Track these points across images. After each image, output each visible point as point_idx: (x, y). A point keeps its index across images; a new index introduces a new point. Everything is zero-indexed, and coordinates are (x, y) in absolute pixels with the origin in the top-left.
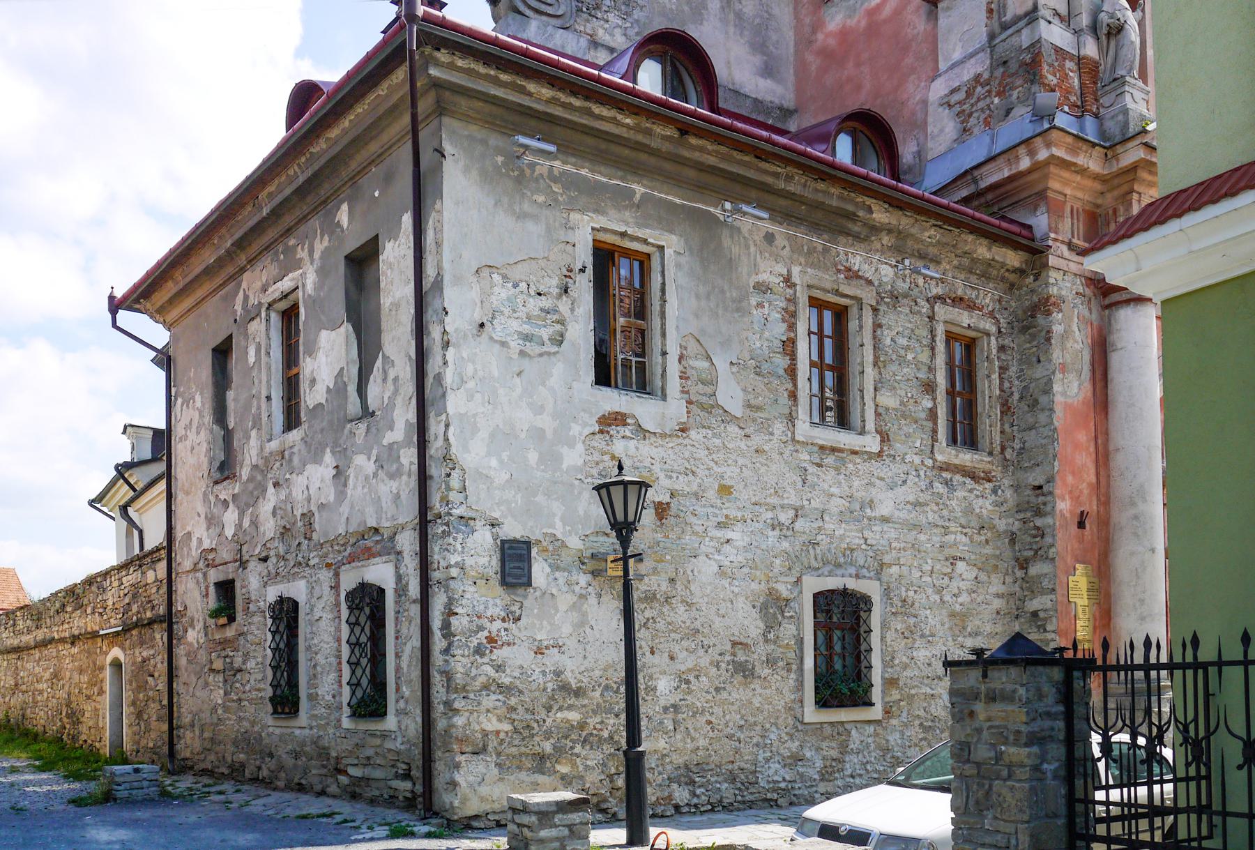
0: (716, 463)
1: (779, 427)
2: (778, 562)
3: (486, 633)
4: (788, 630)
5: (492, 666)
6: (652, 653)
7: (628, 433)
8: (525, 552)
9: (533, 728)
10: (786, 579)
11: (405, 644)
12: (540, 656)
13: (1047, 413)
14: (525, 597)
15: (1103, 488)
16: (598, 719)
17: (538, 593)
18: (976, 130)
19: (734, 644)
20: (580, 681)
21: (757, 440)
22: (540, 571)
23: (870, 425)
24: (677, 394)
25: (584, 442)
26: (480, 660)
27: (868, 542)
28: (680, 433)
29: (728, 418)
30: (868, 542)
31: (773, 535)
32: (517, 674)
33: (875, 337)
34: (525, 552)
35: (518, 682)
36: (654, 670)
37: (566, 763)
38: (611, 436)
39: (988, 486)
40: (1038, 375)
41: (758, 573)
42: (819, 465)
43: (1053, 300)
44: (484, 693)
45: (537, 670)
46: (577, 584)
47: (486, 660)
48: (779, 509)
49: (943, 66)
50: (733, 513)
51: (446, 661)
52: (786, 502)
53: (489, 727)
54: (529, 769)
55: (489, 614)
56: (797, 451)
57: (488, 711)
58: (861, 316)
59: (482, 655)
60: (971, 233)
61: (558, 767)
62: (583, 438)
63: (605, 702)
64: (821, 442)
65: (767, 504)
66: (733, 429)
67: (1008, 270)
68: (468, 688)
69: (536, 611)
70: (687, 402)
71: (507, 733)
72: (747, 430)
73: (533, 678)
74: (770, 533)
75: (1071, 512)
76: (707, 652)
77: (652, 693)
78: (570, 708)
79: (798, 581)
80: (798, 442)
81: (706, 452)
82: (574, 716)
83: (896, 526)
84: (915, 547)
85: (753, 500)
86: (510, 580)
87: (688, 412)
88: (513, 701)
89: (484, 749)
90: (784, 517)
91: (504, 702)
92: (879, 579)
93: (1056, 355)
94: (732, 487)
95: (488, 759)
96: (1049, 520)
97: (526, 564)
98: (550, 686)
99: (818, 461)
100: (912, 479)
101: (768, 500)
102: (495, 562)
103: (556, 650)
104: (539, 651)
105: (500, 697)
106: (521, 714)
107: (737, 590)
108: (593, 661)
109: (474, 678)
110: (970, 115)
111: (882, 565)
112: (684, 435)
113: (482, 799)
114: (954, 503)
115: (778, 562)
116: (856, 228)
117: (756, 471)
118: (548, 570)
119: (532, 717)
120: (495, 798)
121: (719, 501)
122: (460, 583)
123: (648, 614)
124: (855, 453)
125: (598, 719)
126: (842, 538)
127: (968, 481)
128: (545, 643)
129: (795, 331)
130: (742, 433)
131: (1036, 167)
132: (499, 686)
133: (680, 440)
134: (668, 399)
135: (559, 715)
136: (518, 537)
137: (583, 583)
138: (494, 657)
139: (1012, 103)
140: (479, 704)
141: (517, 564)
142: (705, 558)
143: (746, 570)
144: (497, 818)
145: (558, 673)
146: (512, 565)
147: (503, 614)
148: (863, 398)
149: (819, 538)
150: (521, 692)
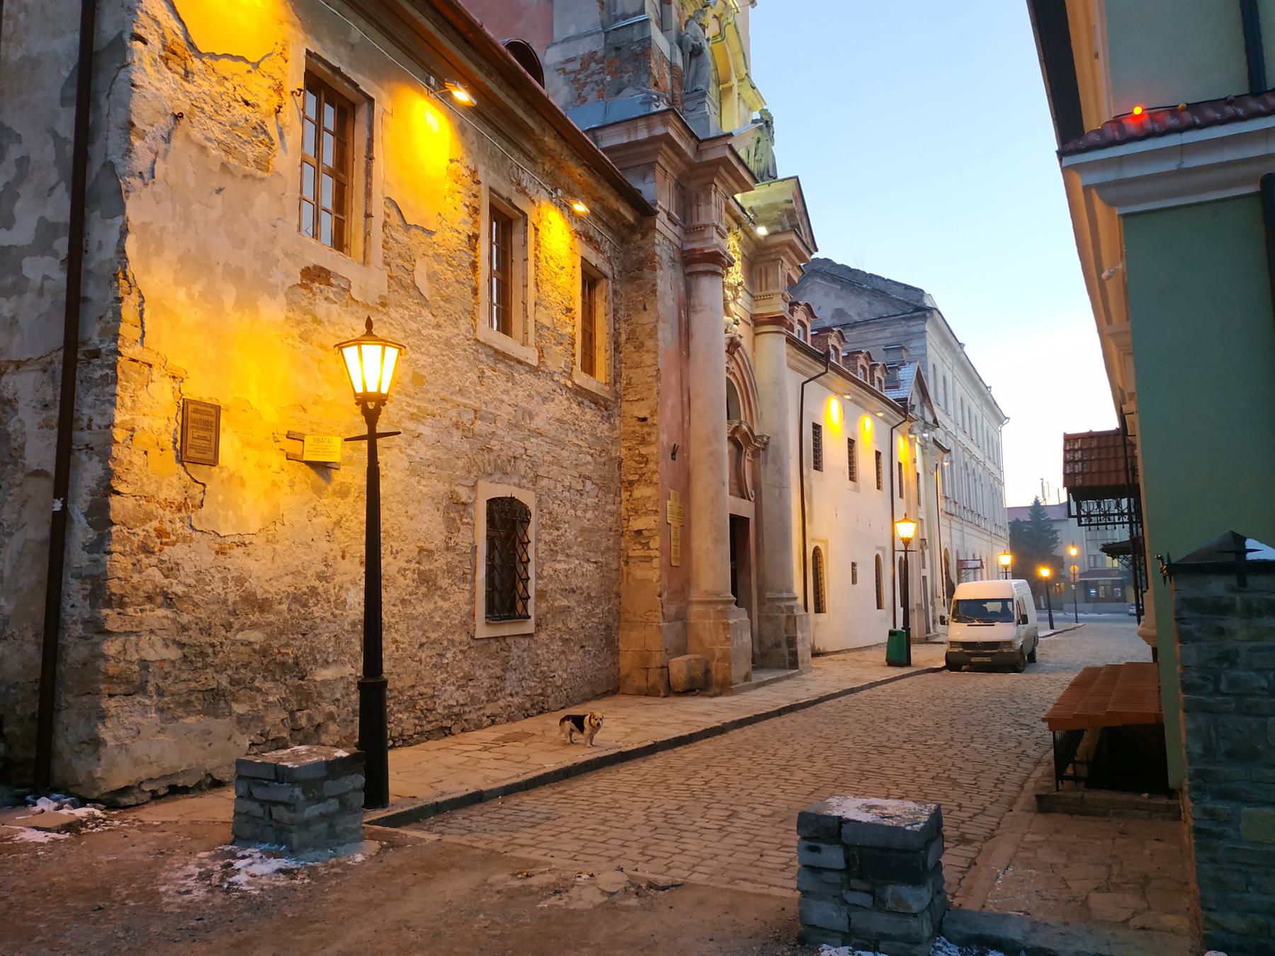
0: (411, 347)
1: (464, 324)
2: (460, 463)
3: (155, 524)
4: (463, 539)
5: (160, 570)
6: (343, 557)
7: (331, 296)
8: (213, 419)
9: (208, 656)
10: (464, 482)
11: (11, 534)
12: (221, 557)
13: (652, 355)
14: (209, 477)
15: (684, 427)
16: (284, 639)
17: (225, 475)
18: (590, 98)
19: (421, 550)
20: (266, 591)
21: (449, 331)
22: (228, 445)
23: (532, 338)
24: (381, 265)
25: (286, 294)
26: (145, 561)
27: (529, 452)
28: (380, 308)
29: (424, 303)
30: (529, 452)
31: (457, 434)
32: (189, 581)
33: (536, 255)
34: (213, 419)
35: (192, 591)
36: (345, 578)
37: (244, 702)
38: (314, 295)
39: (605, 413)
40: (644, 321)
41: (443, 473)
42: (495, 371)
43: (657, 258)
44: (147, 607)
45: (218, 576)
46: (269, 467)
47: (154, 560)
48: (462, 407)
49: (557, 36)
50: (424, 405)
51: (95, 561)
52: (467, 401)
53: (151, 656)
54: (199, 712)
55: (162, 496)
56: (477, 351)
57: (152, 632)
58: (526, 231)
59: (148, 551)
60: (607, 181)
61: (235, 706)
62: (286, 289)
63: (293, 618)
64: (496, 346)
65: (453, 401)
66: (426, 313)
67: (624, 224)
68: (126, 600)
69: (220, 498)
70: (389, 276)
71: (173, 662)
72: (438, 319)
73: (212, 586)
74: (454, 431)
75: (668, 445)
76: (395, 558)
77: (341, 606)
78: (254, 626)
79: (473, 488)
80: (478, 341)
81: (402, 334)
82: (256, 636)
83: (548, 440)
84: (557, 461)
85: (443, 394)
86: (191, 453)
87: (389, 287)
88: (185, 619)
89: (142, 689)
90: (467, 417)
91: (174, 620)
92: (534, 490)
93: (660, 307)
94: (425, 377)
95: (147, 702)
96: (653, 449)
97: (213, 435)
98: (232, 598)
99: (492, 365)
100: (558, 398)
101: (454, 398)
102: (175, 425)
103: (241, 550)
104: (221, 552)
105: (169, 613)
106: (193, 637)
107: (425, 490)
108: (281, 565)
109: (135, 588)
110: (585, 84)
111: (537, 476)
112: (384, 310)
113: (137, 762)
114: (584, 425)
115: (460, 463)
116: (528, 147)
117: (445, 364)
118: (238, 445)
119: (208, 639)
120: (153, 759)
121: (411, 390)
122: (126, 451)
123: (341, 510)
124: (519, 362)
125: (284, 639)
126: (509, 446)
127: (593, 406)
128: (229, 540)
129: (478, 228)
130: (434, 321)
131: (652, 140)
132: (165, 595)
133: (380, 316)
134: (372, 266)
135: (239, 636)
136: (206, 400)
137: (276, 467)
138: (165, 558)
139: (623, 83)
140: (141, 623)
141: (202, 433)
142: (397, 451)
143: (432, 469)
144: (154, 787)
145: (240, 581)
146: (195, 435)
147: (180, 499)
148: (525, 310)
149: (493, 442)
150: (196, 605)
